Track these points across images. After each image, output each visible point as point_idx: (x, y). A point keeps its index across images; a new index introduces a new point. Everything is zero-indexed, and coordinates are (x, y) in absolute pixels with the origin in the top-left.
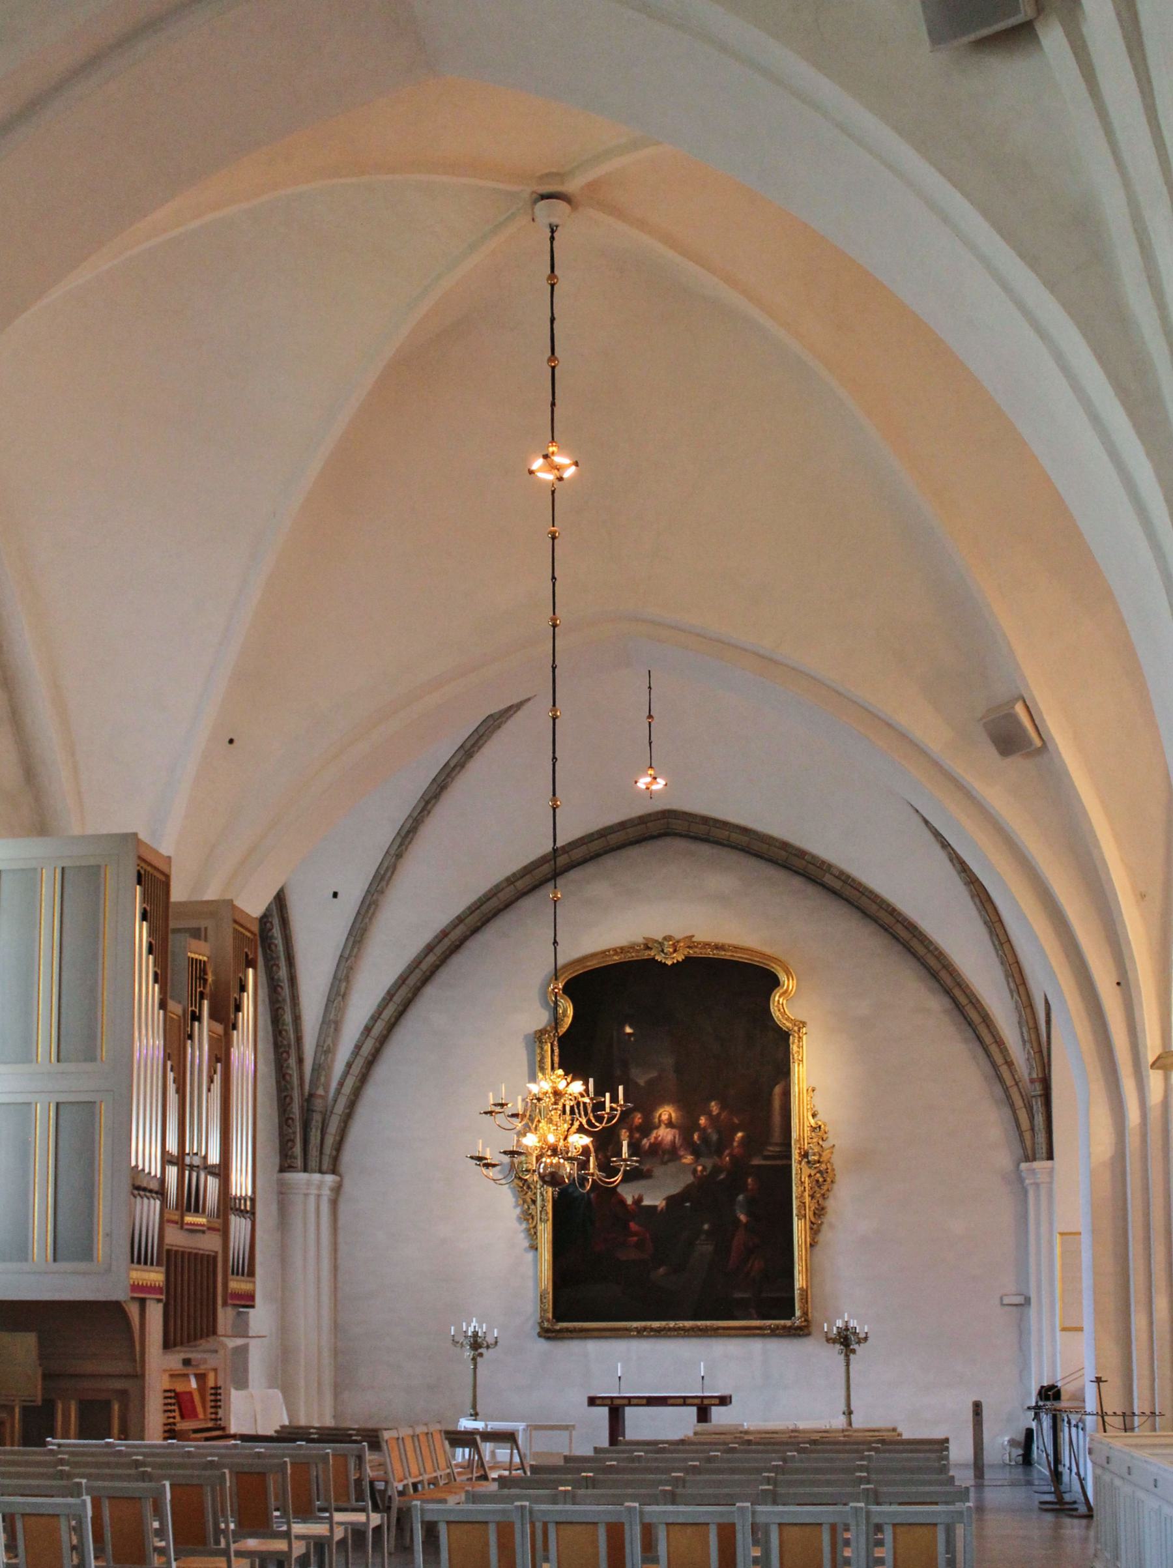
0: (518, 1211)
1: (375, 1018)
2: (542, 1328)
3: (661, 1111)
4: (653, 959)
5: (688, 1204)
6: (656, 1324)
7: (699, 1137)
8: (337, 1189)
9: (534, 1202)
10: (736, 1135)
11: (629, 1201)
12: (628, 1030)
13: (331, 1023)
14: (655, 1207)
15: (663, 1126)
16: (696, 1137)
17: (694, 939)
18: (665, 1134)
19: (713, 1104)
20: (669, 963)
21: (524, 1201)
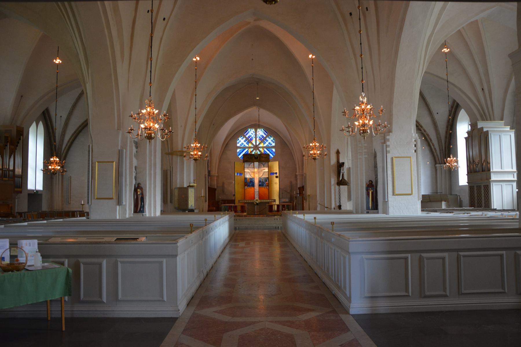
1: (70, 139)
13: (62, 140)
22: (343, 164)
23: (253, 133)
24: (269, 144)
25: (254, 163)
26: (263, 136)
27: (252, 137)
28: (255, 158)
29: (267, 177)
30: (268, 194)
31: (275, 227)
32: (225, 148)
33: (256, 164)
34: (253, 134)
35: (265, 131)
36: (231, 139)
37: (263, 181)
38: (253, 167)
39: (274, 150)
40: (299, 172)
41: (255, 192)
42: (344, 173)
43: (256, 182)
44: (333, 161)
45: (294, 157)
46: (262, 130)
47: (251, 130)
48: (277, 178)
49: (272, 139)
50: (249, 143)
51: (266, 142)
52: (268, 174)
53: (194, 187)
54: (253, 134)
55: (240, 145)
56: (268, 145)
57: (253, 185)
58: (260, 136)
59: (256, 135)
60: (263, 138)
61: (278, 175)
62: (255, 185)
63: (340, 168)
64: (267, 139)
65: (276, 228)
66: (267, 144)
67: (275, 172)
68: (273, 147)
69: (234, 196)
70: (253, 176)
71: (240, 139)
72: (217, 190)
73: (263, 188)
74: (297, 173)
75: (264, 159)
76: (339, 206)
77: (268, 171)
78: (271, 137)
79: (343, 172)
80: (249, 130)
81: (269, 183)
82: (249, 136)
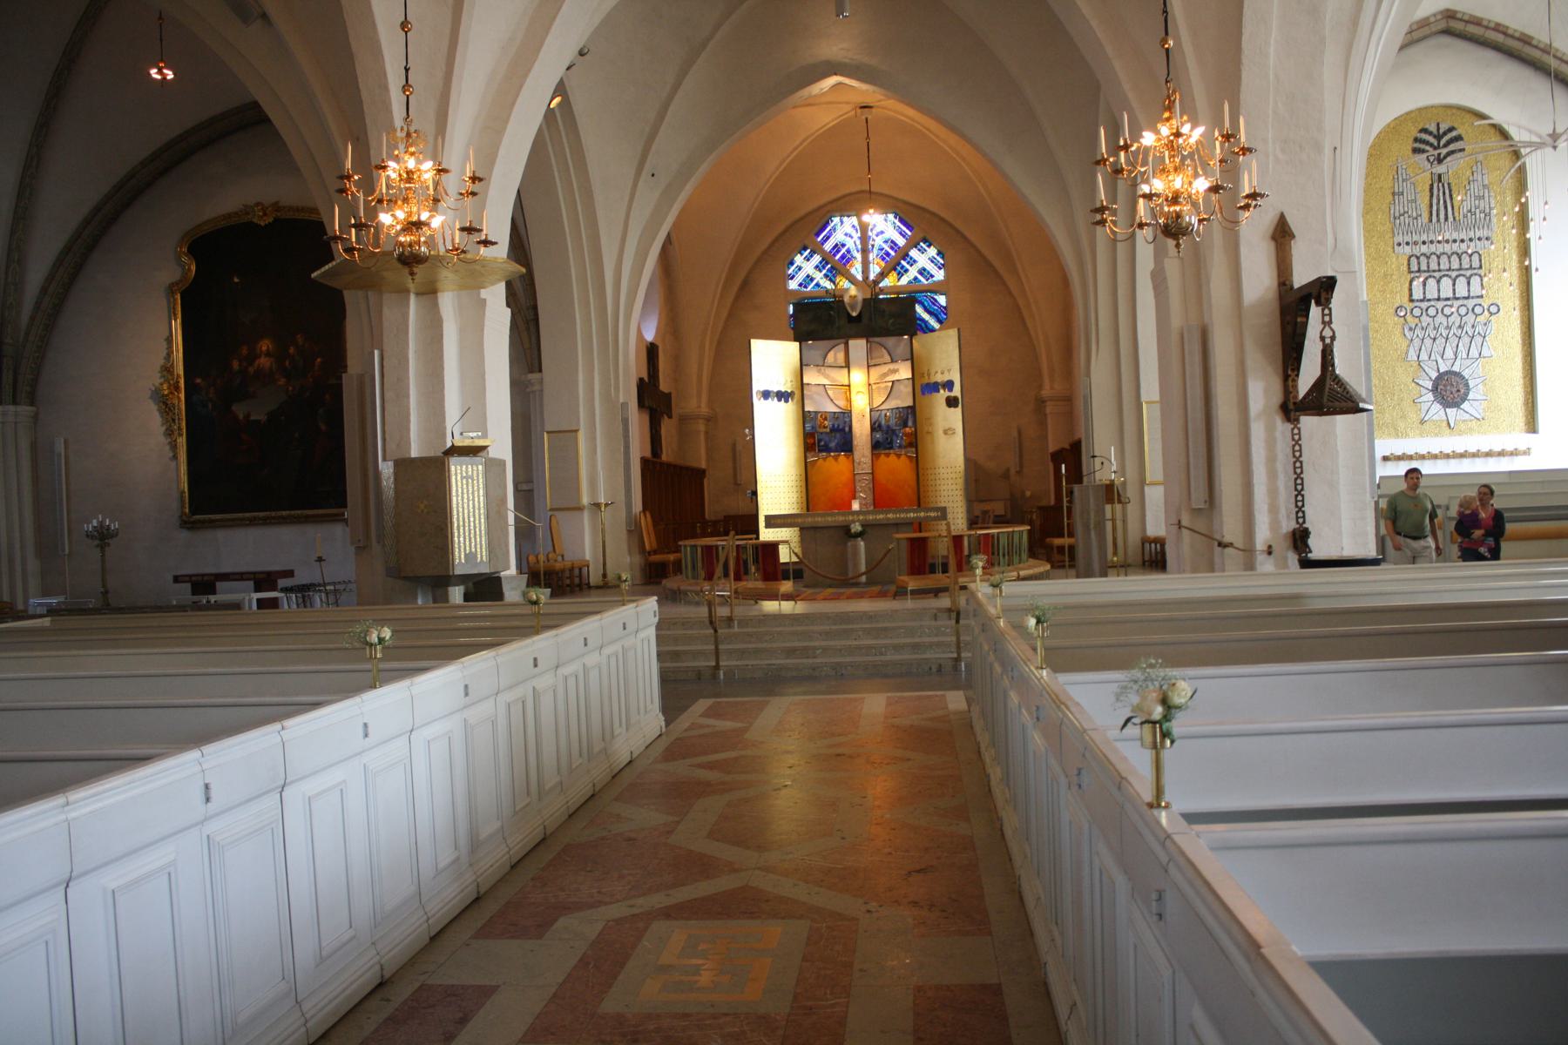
0: (164, 428)
1: (50, 279)
2: (182, 520)
3: (261, 343)
4: (252, 222)
5: (283, 418)
6: (261, 514)
7: (290, 364)
8: (36, 417)
9: (174, 420)
10: (316, 360)
11: (241, 417)
12: (236, 280)
14: (260, 421)
15: (263, 356)
16: (287, 363)
17: (280, 204)
18: (264, 362)
19: (299, 336)
20: (262, 224)
21: (167, 421)
22: (1324, 288)
23: (853, 233)
24: (921, 274)
25: (847, 344)
26: (893, 244)
27: (848, 251)
28: (850, 319)
29: (909, 403)
30: (913, 483)
31: (934, 669)
32: (737, 298)
33: (858, 346)
34: (851, 237)
35: (901, 221)
36: (759, 260)
37: (888, 427)
38: (844, 365)
39: (942, 300)
40: (1052, 388)
41: (857, 477)
42: (1333, 338)
43: (861, 429)
44: (1259, 281)
45: (1029, 324)
46: (891, 216)
47: (845, 219)
48: (952, 409)
49: (932, 251)
50: (834, 276)
51: (907, 266)
52: (910, 389)
53: (483, 454)
54: (851, 237)
55: (800, 285)
56: (916, 278)
57: (847, 445)
58: (882, 243)
59: (864, 239)
60: (896, 251)
61: (957, 392)
62: (855, 443)
63: (1299, 320)
64: (914, 253)
65: (939, 670)
66: (912, 277)
67: (940, 378)
68: (937, 288)
69: (754, 497)
70: (842, 403)
71: (799, 259)
72: (707, 473)
73: (893, 458)
74: (1046, 392)
75: (891, 321)
76: (1294, 533)
77: (913, 378)
78: (929, 246)
79: (1328, 333)
80: (836, 220)
81: (915, 434)
82: (837, 245)
